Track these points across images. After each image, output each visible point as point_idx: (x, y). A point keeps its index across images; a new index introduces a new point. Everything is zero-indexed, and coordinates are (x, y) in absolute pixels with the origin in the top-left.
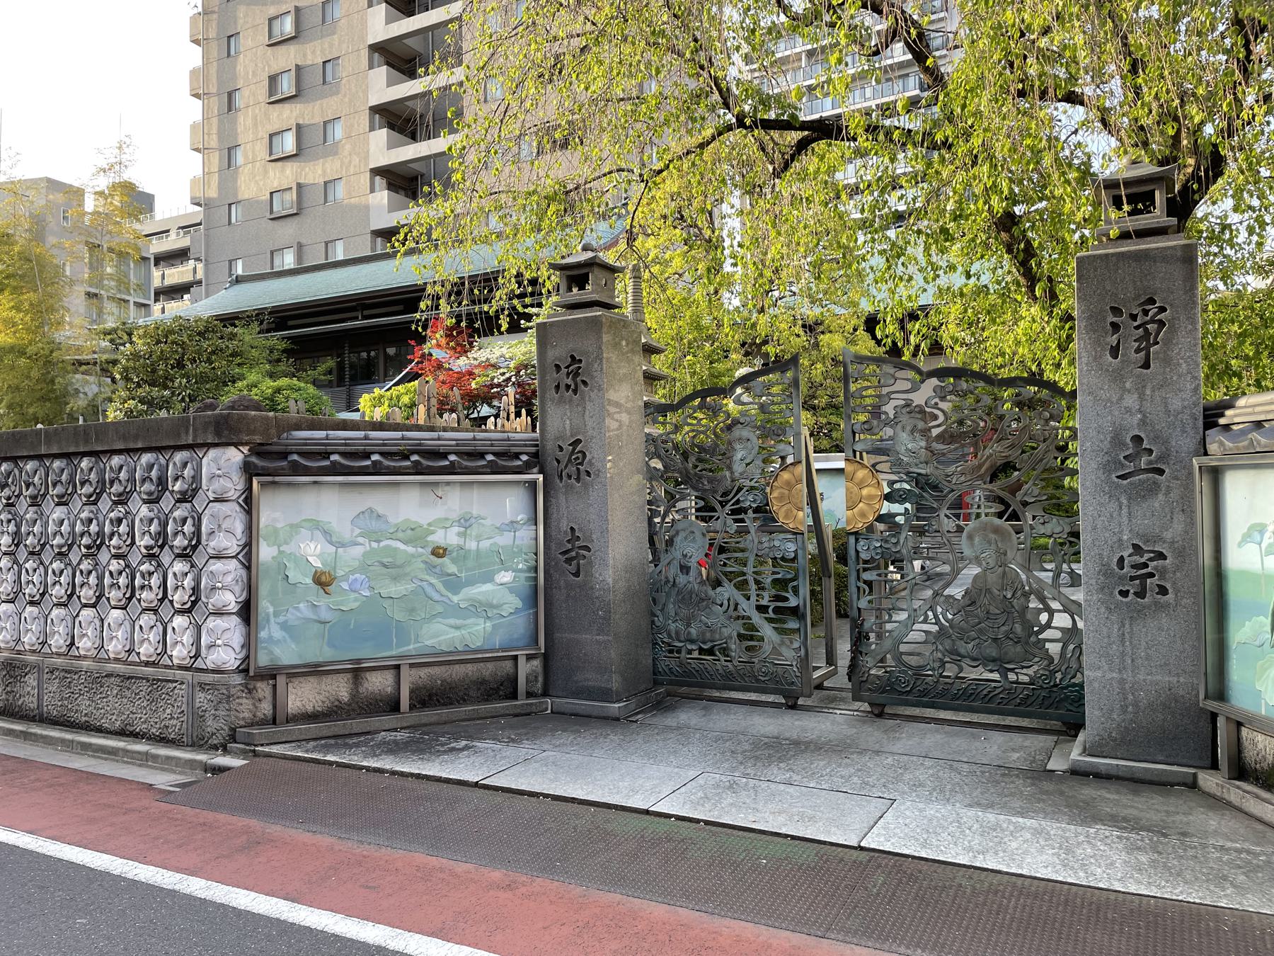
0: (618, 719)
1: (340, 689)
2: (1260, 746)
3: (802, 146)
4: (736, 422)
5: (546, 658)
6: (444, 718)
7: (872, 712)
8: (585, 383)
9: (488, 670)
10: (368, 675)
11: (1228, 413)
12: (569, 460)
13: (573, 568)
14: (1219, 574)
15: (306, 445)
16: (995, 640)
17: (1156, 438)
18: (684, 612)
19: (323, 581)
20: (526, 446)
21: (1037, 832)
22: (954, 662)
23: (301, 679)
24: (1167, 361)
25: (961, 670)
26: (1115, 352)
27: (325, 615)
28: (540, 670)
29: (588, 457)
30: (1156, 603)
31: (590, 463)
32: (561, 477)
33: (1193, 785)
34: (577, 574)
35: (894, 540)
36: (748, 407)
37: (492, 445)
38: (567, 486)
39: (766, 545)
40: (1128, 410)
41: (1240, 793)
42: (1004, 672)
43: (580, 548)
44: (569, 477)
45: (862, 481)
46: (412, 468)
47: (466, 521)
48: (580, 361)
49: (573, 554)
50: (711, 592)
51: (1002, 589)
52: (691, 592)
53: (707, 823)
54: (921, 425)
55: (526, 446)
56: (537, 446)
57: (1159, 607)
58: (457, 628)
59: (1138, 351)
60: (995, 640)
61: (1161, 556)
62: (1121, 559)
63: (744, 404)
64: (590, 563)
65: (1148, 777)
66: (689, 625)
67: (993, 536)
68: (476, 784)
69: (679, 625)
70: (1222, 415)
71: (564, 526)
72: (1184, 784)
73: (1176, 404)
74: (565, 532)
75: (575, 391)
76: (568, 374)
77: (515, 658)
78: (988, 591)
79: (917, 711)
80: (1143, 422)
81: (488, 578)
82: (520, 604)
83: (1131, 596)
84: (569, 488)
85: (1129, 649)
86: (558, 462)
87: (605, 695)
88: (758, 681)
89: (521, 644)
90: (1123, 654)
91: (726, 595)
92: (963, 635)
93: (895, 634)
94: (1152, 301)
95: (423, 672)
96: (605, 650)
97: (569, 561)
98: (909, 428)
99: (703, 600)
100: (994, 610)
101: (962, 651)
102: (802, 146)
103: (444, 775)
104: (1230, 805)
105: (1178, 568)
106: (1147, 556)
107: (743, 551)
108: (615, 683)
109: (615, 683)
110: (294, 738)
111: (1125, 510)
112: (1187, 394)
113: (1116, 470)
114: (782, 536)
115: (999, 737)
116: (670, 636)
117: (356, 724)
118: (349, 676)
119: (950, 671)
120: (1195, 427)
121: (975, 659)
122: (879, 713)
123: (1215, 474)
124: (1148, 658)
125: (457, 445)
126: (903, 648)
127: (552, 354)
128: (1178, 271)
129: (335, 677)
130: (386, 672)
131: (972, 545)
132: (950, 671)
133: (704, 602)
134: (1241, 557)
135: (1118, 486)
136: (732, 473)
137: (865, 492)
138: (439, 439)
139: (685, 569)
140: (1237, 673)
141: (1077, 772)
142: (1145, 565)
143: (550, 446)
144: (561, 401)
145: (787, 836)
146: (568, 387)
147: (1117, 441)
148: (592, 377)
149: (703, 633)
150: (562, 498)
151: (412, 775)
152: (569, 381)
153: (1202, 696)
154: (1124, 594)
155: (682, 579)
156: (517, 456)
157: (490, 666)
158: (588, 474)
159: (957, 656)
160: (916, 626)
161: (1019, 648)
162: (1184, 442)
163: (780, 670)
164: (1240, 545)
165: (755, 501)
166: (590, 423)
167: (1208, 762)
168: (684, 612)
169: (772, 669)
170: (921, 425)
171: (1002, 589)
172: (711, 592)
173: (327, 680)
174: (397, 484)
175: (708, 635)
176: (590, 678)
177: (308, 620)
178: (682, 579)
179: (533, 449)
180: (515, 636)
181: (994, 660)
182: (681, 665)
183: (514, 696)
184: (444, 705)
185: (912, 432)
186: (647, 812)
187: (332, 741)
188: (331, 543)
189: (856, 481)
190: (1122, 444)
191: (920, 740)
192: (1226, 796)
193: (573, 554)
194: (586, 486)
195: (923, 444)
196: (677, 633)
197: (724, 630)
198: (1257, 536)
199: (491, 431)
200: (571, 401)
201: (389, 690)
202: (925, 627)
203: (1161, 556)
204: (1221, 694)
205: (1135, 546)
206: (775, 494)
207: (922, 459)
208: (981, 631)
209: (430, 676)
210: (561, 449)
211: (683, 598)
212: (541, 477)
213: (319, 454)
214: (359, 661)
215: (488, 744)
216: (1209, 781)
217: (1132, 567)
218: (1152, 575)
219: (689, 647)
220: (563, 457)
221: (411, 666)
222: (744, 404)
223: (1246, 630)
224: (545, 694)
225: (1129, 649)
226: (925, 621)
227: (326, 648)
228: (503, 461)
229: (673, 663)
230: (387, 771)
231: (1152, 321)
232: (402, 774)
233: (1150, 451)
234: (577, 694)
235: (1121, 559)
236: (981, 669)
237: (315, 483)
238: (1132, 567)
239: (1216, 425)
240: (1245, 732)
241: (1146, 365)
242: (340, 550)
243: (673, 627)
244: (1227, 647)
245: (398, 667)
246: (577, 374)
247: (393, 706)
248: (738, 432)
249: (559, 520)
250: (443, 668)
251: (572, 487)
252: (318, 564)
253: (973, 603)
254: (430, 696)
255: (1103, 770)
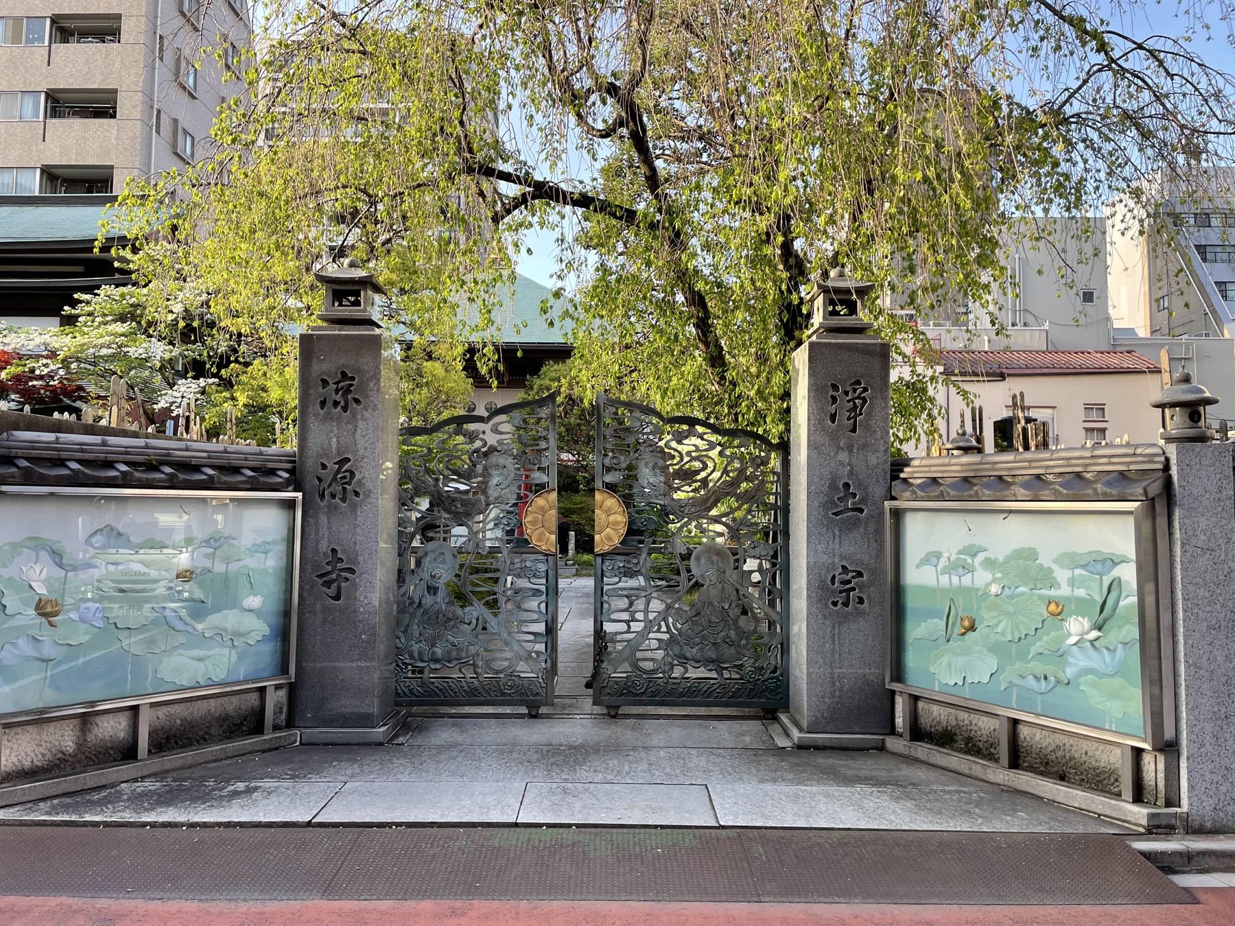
0: (381, 744)
1: (65, 739)
2: (935, 714)
3: (521, 201)
4: (493, 450)
5: (292, 689)
6: (190, 761)
7: (609, 714)
8: (357, 401)
9: (231, 705)
10: (98, 719)
11: (906, 469)
12: (334, 479)
13: (332, 591)
14: (898, 590)
15: (34, 448)
16: (714, 644)
17: (860, 485)
18: (429, 632)
19: (46, 610)
20: (281, 461)
21: (827, 796)
22: (681, 664)
23: (19, 730)
24: (868, 428)
25: (686, 670)
26: (833, 418)
27: (48, 651)
28: (285, 700)
29: (358, 476)
30: (856, 609)
31: (360, 482)
32: (322, 496)
33: (881, 748)
34: (337, 597)
35: (635, 561)
36: (504, 437)
37: (246, 459)
38: (329, 506)
39: (518, 565)
40: (841, 463)
41: (922, 750)
42: (720, 670)
43: (341, 570)
44: (333, 496)
45: (609, 509)
46: (167, 481)
47: (216, 541)
48: (353, 379)
49: (334, 576)
50: (459, 612)
51: (722, 601)
52: (438, 613)
53: (578, 826)
54: (661, 463)
55: (281, 461)
56: (294, 462)
57: (860, 614)
58: (200, 660)
59: (849, 419)
60: (714, 644)
61: (860, 574)
62: (834, 577)
63: (502, 433)
64: (355, 586)
65: (851, 745)
66: (434, 645)
67: (715, 558)
68: (309, 824)
69: (423, 645)
70: (902, 471)
71: (324, 546)
72: (876, 748)
73: (873, 460)
74: (325, 554)
75: (345, 409)
76: (337, 391)
77: (262, 690)
78: (711, 603)
79: (651, 710)
80: (851, 473)
81: (234, 604)
82: (267, 631)
83: (839, 605)
84: (332, 509)
85: (837, 648)
86: (320, 480)
87: (365, 720)
88: (503, 694)
89: (265, 674)
90: (833, 650)
91: (475, 614)
92: (689, 642)
93: (632, 643)
94: (858, 383)
95: (162, 712)
96: (361, 675)
97: (327, 584)
98: (650, 465)
99: (450, 620)
100: (714, 619)
101: (689, 655)
102: (521, 201)
103: (263, 819)
104: (917, 761)
105: (871, 583)
106: (850, 575)
107: (497, 570)
108: (373, 706)
109: (375, 710)
110: (16, 800)
111: (837, 540)
112: (881, 454)
113: (831, 508)
114: (533, 557)
115: (723, 726)
116: (412, 657)
117: (90, 778)
118: (76, 722)
119: (677, 672)
120: (885, 478)
121: (698, 661)
122: (613, 714)
123: (898, 515)
124: (850, 652)
125: (209, 457)
126: (639, 655)
127: (317, 368)
128: (877, 363)
129: (58, 724)
130: (120, 714)
131: (699, 564)
132: (677, 672)
133: (450, 622)
134: (916, 575)
135: (833, 521)
136: (487, 497)
137: (611, 518)
138: (187, 450)
139: (432, 590)
140: (912, 660)
141: (801, 747)
142: (849, 582)
143: (310, 463)
144: (327, 418)
145: (656, 827)
146: (336, 404)
147: (833, 486)
148: (367, 396)
149: (449, 653)
150: (323, 519)
151: (219, 824)
152: (338, 398)
153: (887, 679)
154: (835, 604)
155: (428, 600)
156: (273, 472)
157: (235, 700)
158: (357, 494)
159: (684, 660)
160: (651, 635)
161: (732, 650)
162: (878, 490)
163: (526, 683)
164: (918, 567)
165: (508, 525)
166: (361, 443)
167: (888, 731)
168: (429, 632)
169: (518, 681)
170: (661, 463)
171: (722, 601)
172: (459, 612)
173: (51, 728)
174: (90, 498)
175: (454, 654)
176: (347, 704)
177: (28, 659)
178: (428, 600)
179: (289, 466)
180: (261, 666)
181: (713, 661)
182: (423, 685)
183: (258, 729)
184: (183, 746)
185: (654, 468)
186: (516, 825)
187: (68, 800)
188: (60, 566)
189: (604, 507)
190: (837, 488)
191: (664, 733)
192: (913, 754)
193: (334, 576)
194: (354, 507)
195: (662, 479)
196: (420, 653)
197: (471, 648)
198: (934, 560)
199: (170, 439)
200: (339, 419)
201: (122, 735)
202: (660, 636)
203: (860, 574)
204: (898, 674)
205: (844, 567)
206: (529, 518)
207: (662, 492)
208: (704, 637)
209: (169, 715)
210: (324, 466)
211: (429, 618)
212: (299, 495)
213: (50, 460)
214: (92, 703)
215: (267, 784)
216: (892, 743)
217: (842, 583)
218: (853, 589)
219: (433, 666)
220: (327, 475)
221: (152, 705)
222: (502, 433)
223: (917, 631)
224: (290, 724)
225: (837, 648)
226: (658, 631)
227: (47, 690)
228: (261, 476)
229: (414, 684)
230: (182, 824)
231: (859, 397)
232: (205, 825)
233: (854, 495)
234: (331, 722)
235: (834, 577)
236: (702, 669)
237: (52, 494)
238: (842, 583)
239: (898, 478)
240: (921, 705)
241: (854, 430)
242: (70, 574)
243: (416, 647)
244: (904, 642)
245: (135, 709)
246: (347, 391)
247: (128, 752)
248: (493, 459)
249: (317, 542)
250: (183, 706)
251: (336, 507)
252: (41, 590)
253: (698, 614)
254: (168, 738)
255: (820, 743)
